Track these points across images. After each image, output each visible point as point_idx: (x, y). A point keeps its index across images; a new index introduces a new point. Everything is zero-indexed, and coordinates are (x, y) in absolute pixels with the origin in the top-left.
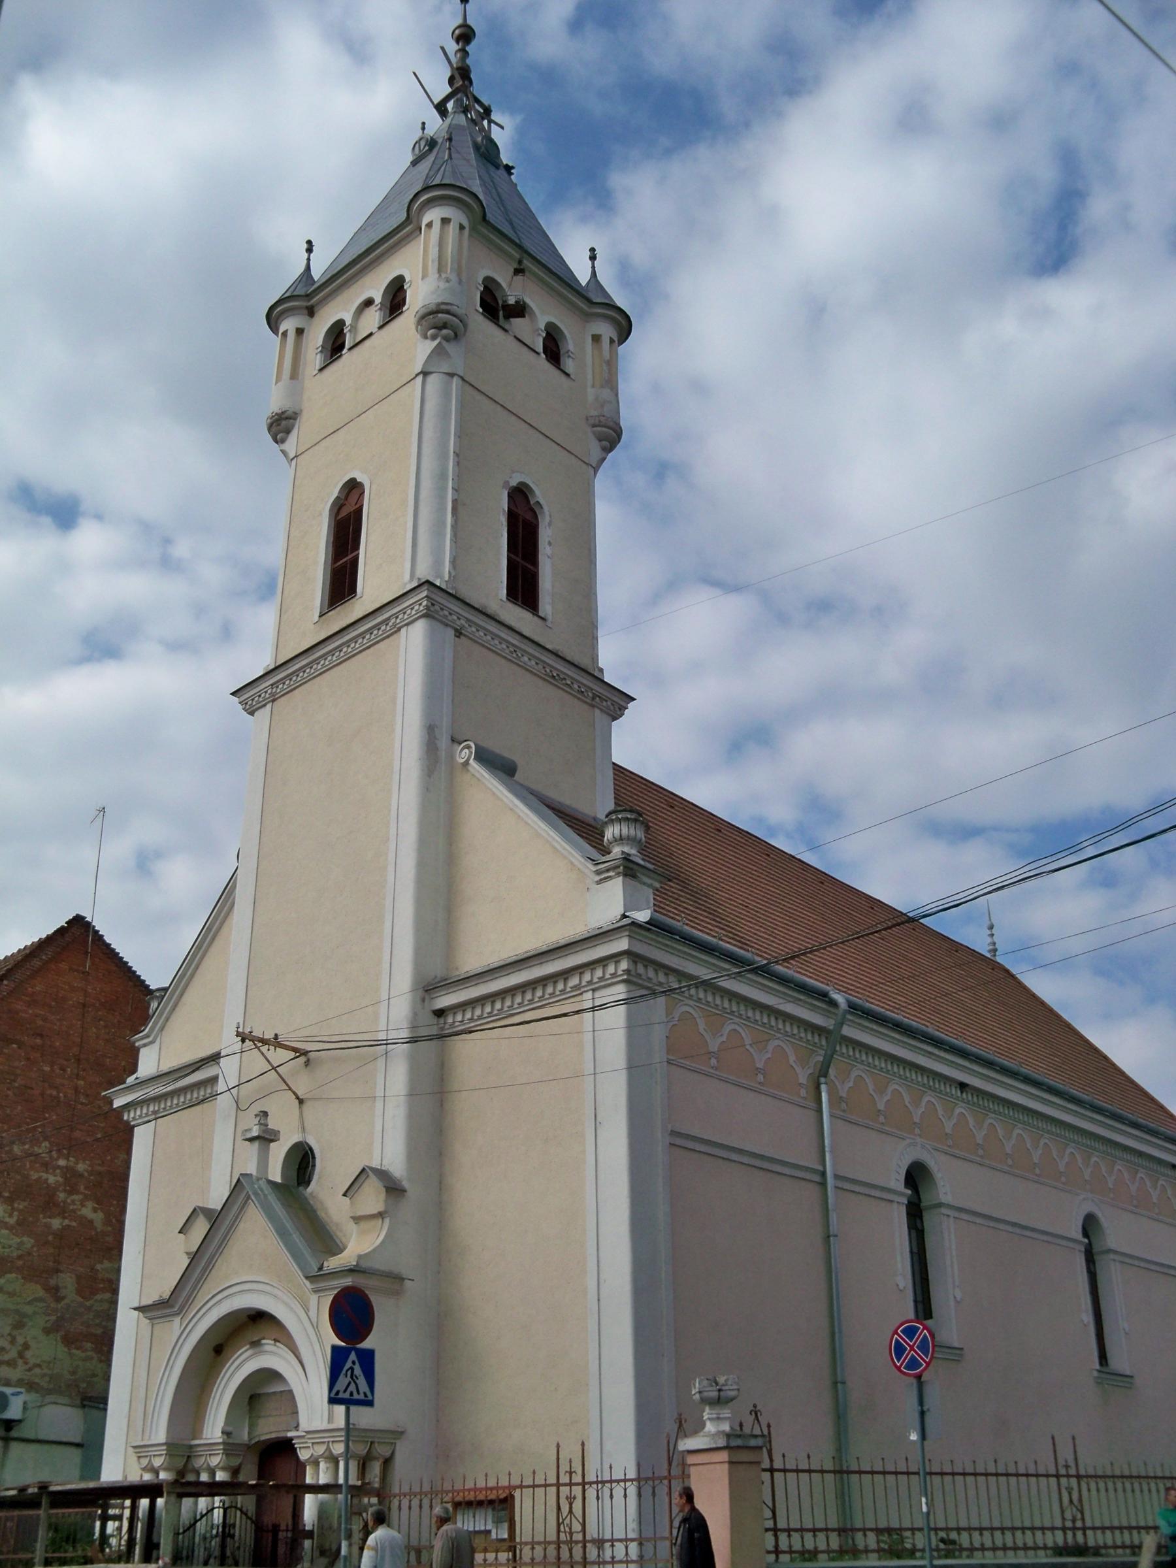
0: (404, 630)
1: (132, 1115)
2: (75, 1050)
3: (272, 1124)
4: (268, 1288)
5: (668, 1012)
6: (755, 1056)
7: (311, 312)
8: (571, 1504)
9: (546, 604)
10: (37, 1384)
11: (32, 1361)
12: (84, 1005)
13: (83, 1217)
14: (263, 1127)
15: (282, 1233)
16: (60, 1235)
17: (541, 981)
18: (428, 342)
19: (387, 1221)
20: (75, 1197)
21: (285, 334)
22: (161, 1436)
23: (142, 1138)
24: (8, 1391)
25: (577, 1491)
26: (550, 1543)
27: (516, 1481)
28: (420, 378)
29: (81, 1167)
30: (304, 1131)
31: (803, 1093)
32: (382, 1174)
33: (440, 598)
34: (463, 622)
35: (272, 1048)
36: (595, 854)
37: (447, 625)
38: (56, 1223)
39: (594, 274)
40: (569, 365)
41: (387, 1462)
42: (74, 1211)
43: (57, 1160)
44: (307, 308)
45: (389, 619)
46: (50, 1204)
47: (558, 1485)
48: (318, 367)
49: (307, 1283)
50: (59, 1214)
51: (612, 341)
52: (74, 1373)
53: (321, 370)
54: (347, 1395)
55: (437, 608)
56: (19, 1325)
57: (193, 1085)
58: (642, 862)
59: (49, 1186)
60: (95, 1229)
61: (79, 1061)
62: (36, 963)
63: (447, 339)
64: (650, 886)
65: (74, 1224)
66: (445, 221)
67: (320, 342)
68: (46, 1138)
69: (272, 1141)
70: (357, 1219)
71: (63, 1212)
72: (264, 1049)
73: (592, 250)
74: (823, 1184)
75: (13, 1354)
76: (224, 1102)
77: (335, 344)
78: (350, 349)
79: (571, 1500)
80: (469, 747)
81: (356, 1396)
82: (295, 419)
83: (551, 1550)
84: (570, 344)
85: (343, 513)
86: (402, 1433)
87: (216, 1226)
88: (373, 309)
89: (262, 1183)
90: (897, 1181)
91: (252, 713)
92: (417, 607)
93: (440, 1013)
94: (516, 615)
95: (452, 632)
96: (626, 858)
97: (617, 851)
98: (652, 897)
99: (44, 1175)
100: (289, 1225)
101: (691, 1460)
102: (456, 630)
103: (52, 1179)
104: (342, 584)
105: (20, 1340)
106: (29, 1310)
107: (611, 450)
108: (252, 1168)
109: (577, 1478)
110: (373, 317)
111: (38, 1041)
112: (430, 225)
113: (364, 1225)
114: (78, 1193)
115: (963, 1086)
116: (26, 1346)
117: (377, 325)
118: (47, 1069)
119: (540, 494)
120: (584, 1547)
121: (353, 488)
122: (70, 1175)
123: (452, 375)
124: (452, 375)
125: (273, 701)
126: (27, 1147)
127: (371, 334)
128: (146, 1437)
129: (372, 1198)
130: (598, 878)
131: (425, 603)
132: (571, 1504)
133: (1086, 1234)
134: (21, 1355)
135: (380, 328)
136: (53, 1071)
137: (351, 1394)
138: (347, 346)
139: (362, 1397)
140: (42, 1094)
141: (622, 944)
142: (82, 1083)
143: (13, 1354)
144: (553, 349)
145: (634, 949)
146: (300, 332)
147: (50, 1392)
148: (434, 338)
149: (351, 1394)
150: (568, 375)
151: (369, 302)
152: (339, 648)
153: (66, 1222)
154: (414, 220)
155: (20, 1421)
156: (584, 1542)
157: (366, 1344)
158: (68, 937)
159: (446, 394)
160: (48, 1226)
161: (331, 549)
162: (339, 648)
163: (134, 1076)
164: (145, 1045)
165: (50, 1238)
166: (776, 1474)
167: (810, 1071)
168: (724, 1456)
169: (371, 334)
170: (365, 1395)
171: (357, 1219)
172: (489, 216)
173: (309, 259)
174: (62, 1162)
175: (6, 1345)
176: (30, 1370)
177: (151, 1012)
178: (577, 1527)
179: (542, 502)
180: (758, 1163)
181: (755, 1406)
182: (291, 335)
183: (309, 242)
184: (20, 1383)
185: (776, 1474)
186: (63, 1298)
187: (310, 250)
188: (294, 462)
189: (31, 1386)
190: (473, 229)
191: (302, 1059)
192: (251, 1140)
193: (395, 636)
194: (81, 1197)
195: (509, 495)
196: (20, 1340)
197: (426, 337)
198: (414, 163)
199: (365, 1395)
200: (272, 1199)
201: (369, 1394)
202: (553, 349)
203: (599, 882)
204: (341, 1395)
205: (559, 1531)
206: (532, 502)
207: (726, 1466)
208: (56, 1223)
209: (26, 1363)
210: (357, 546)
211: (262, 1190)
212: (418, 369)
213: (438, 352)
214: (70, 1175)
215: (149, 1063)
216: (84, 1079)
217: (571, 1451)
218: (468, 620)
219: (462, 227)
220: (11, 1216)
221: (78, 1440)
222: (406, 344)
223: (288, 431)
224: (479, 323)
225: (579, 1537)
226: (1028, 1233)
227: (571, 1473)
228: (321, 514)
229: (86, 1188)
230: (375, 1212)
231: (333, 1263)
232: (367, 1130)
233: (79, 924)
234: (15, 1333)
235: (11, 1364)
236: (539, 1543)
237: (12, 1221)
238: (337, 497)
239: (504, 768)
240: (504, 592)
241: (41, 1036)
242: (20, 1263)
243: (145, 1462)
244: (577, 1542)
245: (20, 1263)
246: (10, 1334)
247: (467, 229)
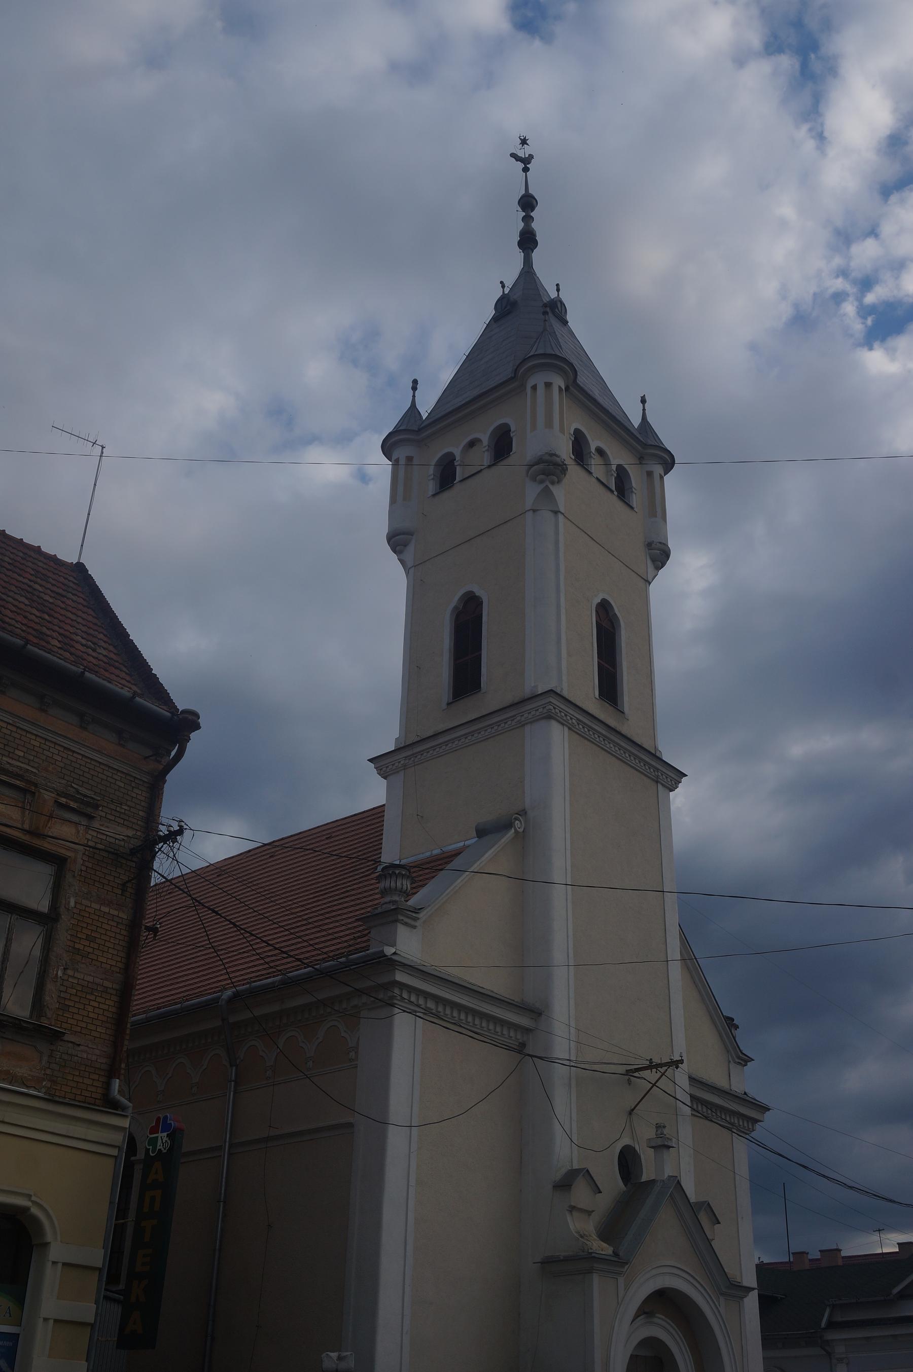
21: (397, 460)
48: (430, 493)
53: (434, 495)
63: (553, 483)
77: (446, 476)
91: (385, 778)
104: (466, 678)
110: (482, 456)
138: (458, 479)
146: (409, 459)
148: (542, 482)
150: (632, 508)
182: (402, 461)
187: (414, 388)
188: (412, 571)
197: (534, 479)
198: (495, 319)
202: (621, 487)
210: (479, 648)
223: (405, 545)
238: (456, 608)
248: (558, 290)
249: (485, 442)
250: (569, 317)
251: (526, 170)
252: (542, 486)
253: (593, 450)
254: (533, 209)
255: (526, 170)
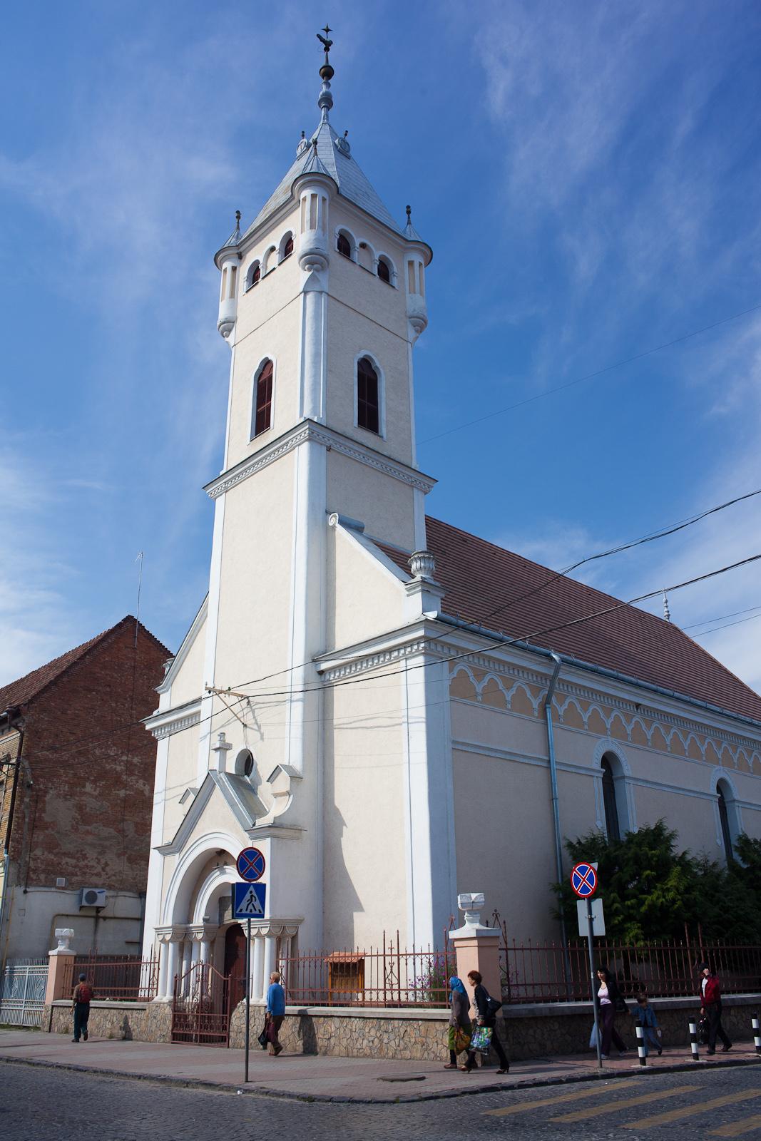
0: (296, 448)
1: (156, 733)
2: (130, 693)
3: (228, 740)
4: (225, 837)
5: (451, 670)
6: (505, 693)
7: (240, 256)
8: (392, 967)
9: (383, 428)
10: (114, 886)
11: (111, 873)
12: (134, 667)
13: (136, 789)
14: (222, 742)
15: (232, 804)
16: (125, 800)
17: (376, 654)
18: (307, 272)
19: (292, 796)
20: (133, 778)
21: (225, 270)
22: (169, 923)
23: (162, 746)
24: (96, 891)
25: (395, 959)
26: (380, 990)
27: (361, 951)
28: (303, 294)
29: (136, 760)
30: (246, 743)
31: (536, 714)
32: (289, 769)
33: (317, 429)
34: (331, 442)
35: (227, 695)
36: (405, 577)
37: (321, 444)
38: (122, 793)
39: (409, 223)
40: (395, 281)
41: (294, 938)
42: (131, 785)
43: (121, 757)
44: (237, 253)
45: (288, 442)
46: (118, 782)
47: (384, 955)
48: (245, 290)
49: (246, 834)
50: (123, 788)
51: (420, 264)
52: (134, 879)
53: (247, 292)
54: (248, 912)
55: (315, 434)
56: (102, 853)
57: (187, 717)
58: (432, 582)
59: (117, 772)
60: (145, 795)
61: (132, 699)
62: (105, 644)
64: (437, 596)
65: (131, 793)
66: (314, 196)
67: (246, 275)
68: (114, 745)
69: (228, 750)
70: (276, 795)
71: (125, 786)
72: (222, 695)
73: (408, 207)
74: (549, 768)
75: (99, 869)
76: (204, 728)
78: (263, 278)
79: (392, 964)
80: (335, 516)
81: (254, 912)
82: (234, 322)
83: (381, 993)
84: (395, 268)
85: (262, 379)
86: (302, 921)
87: (199, 801)
88: (275, 252)
89: (222, 775)
90: (596, 764)
92: (303, 435)
93: (321, 673)
94: (365, 436)
95: (325, 448)
96: (423, 581)
97: (418, 577)
98: (440, 605)
99: (114, 767)
100: (236, 800)
101: (456, 944)
102: (327, 447)
103: (119, 768)
104: (262, 422)
105: (103, 861)
106: (107, 843)
107: (421, 332)
108: (216, 766)
109: (395, 952)
110: (275, 257)
111: (108, 689)
112: (304, 199)
113: (279, 798)
114: (135, 775)
115: (638, 706)
116: (107, 864)
117: (277, 263)
118: (114, 705)
119: (377, 362)
120: (399, 993)
121: (267, 364)
122: (129, 765)
123: (321, 292)
124: (321, 292)
125: (226, 492)
126: (103, 750)
127: (274, 269)
128: (161, 923)
129: (283, 782)
130: (408, 593)
131: (307, 432)
132: (392, 967)
133: (719, 790)
134: (103, 869)
135: (279, 265)
136: (117, 706)
137: (251, 911)
138: (261, 277)
139: (257, 912)
140: (111, 720)
141: (421, 633)
142: (134, 712)
143: (99, 869)
144: (384, 272)
145: (428, 635)
146: (234, 269)
147: (122, 890)
149: (251, 911)
151: (273, 249)
152: (261, 460)
153: (128, 792)
154: (296, 197)
155: (104, 907)
156: (399, 990)
157: (261, 880)
158: (123, 629)
159: (317, 304)
160: (118, 795)
161: (256, 399)
162: (261, 460)
163: (157, 711)
164: (163, 693)
165: (119, 801)
166: (509, 952)
167: (541, 700)
168: (475, 943)
169: (274, 269)
170: (260, 911)
171: (276, 795)
172: (341, 191)
173: (238, 223)
174: (124, 758)
175: (95, 864)
176: (109, 878)
177: (166, 673)
178: (395, 981)
179: (378, 365)
180: (508, 757)
181: (496, 911)
183: (238, 212)
184: (103, 886)
185: (509, 952)
186: (127, 836)
189: (110, 887)
190: (331, 200)
191: (246, 700)
192: (216, 750)
193: (292, 452)
194: (136, 777)
195: (358, 363)
196: (103, 861)
199: (260, 911)
200: (227, 784)
201: (262, 911)
202: (384, 272)
203: (408, 596)
204: (244, 912)
205: (385, 983)
206: (373, 367)
207: (477, 948)
208: (122, 793)
209: (107, 874)
211: (221, 779)
212: (301, 290)
213: (312, 279)
214: (129, 765)
215: (165, 703)
216: (136, 709)
217: (391, 936)
218: (334, 440)
219: (324, 199)
220: (95, 791)
221: (136, 916)
222: (294, 274)
223: (230, 331)
224: (337, 259)
225: (396, 987)
226: (681, 792)
227: (391, 949)
228: (249, 379)
229: (139, 772)
230: (284, 791)
231: (261, 822)
232: (281, 744)
233: (130, 620)
234: (99, 857)
235: (98, 875)
236: (374, 990)
237: (96, 793)
239: (355, 528)
240: (357, 422)
241: (109, 686)
242: (101, 817)
243: (161, 937)
244: (395, 990)
245: (101, 817)
246: (97, 858)
247: (327, 202)
248: (346, 135)
249: (277, 248)
250: (351, 153)
251: (327, 49)
252: (311, 273)
253: (357, 245)
254: (330, 78)
255: (327, 49)
